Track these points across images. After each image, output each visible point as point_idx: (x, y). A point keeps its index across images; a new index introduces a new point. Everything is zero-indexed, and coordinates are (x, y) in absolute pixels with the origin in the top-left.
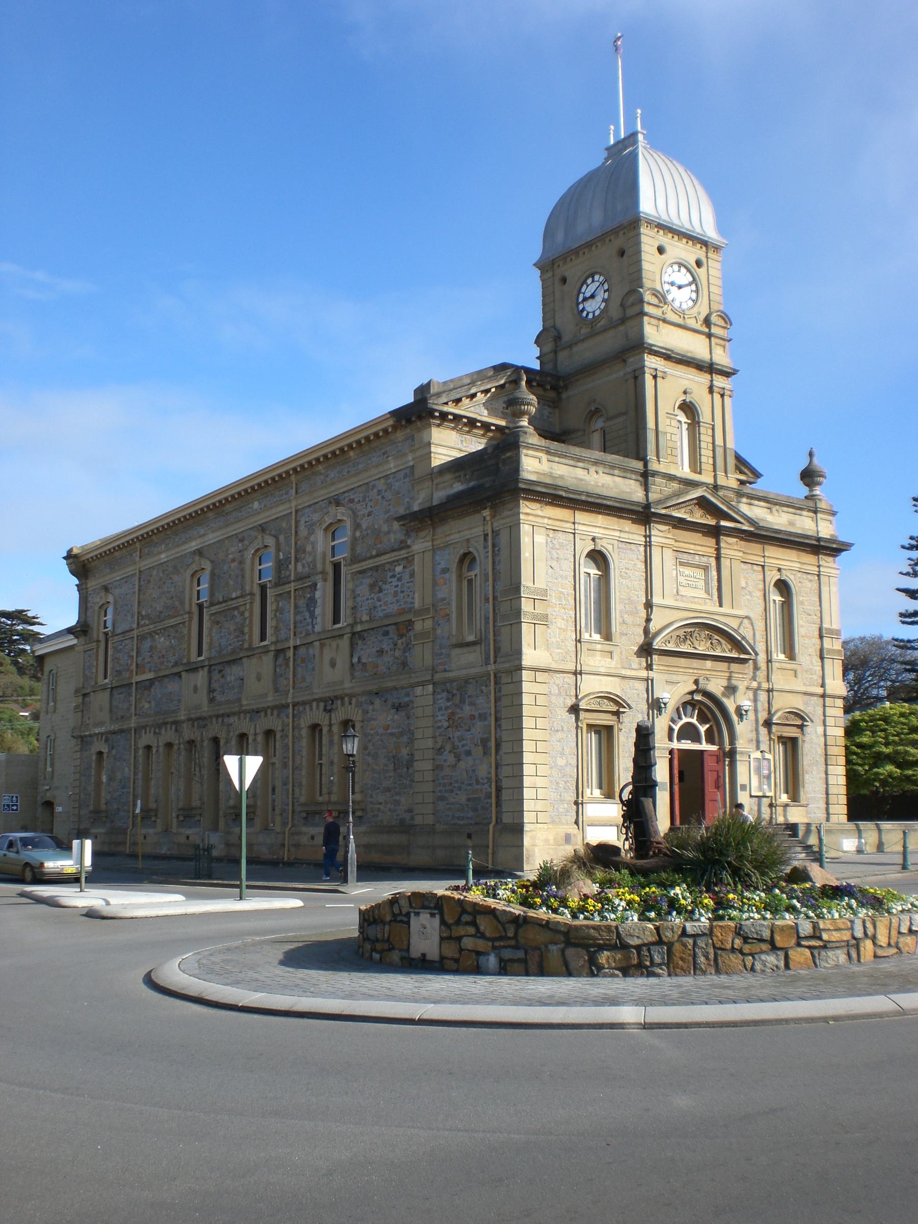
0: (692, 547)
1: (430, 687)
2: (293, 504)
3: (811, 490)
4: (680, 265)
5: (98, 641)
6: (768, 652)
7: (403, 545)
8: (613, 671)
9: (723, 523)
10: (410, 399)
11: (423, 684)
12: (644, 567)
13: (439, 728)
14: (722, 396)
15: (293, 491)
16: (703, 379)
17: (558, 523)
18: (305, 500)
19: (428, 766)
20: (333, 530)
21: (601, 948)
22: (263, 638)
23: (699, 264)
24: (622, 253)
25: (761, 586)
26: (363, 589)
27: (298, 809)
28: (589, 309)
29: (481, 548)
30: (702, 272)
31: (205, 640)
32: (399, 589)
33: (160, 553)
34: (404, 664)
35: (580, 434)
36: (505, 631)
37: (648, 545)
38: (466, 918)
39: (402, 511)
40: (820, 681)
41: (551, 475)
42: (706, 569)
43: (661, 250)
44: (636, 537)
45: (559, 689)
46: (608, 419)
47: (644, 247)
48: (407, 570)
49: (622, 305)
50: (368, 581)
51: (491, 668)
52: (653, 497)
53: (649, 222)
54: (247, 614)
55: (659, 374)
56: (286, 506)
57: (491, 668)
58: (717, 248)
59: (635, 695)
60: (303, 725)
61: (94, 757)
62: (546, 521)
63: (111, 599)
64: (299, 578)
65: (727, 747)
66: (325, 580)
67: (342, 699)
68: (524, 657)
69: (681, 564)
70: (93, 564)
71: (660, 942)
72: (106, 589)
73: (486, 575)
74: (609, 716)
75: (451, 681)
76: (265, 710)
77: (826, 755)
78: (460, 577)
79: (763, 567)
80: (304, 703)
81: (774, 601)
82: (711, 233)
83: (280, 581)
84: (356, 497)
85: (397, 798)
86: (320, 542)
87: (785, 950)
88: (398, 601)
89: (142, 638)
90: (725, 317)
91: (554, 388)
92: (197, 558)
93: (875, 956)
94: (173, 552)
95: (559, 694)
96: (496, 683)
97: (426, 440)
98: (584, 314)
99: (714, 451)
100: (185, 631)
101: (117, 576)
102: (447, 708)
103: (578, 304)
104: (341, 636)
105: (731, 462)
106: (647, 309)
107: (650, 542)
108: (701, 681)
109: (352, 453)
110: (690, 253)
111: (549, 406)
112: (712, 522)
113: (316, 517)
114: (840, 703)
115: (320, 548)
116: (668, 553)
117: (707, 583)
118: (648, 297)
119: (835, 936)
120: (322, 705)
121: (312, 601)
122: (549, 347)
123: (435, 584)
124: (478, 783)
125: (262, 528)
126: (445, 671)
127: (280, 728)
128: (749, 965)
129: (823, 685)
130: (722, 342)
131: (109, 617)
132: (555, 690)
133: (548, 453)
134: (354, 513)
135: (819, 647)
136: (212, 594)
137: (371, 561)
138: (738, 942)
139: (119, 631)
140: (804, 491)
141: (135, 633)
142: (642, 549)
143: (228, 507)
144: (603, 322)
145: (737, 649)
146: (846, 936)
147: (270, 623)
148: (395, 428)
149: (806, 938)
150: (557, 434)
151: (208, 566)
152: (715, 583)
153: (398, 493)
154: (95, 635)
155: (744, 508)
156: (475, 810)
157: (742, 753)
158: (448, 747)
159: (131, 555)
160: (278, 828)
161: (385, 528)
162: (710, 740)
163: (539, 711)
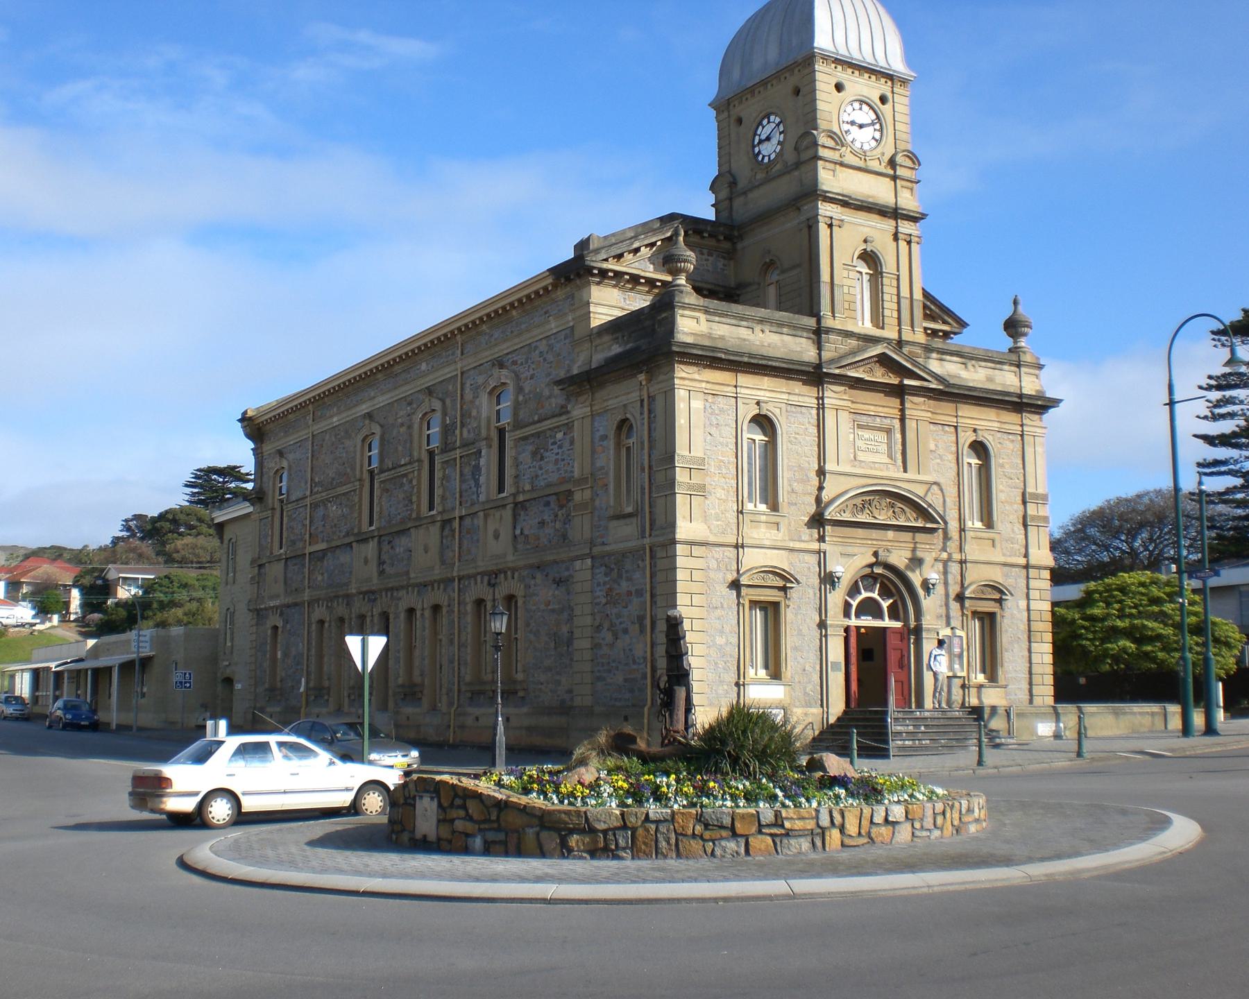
1: (589, 561)
2: (459, 365)
3: (1015, 342)
4: (862, 102)
5: (273, 509)
6: (961, 520)
7: (563, 411)
8: (779, 544)
9: (906, 382)
10: (569, 254)
11: (582, 558)
13: (597, 604)
14: (909, 243)
15: (459, 352)
16: (888, 225)
17: (717, 387)
18: (470, 362)
19: (586, 644)
20: (497, 394)
21: (571, 832)
22: (431, 508)
23: (883, 100)
24: (797, 92)
25: (954, 449)
26: (526, 457)
27: (463, 688)
28: (764, 152)
29: (638, 416)
30: (887, 109)
31: (376, 509)
32: (559, 457)
33: (332, 417)
34: (564, 537)
35: (754, 287)
36: (660, 503)
37: (821, 407)
38: (458, 802)
39: (562, 374)
40: (1023, 551)
41: (710, 336)
42: (889, 431)
43: (839, 87)
44: (807, 399)
45: (718, 563)
46: (783, 272)
47: (819, 85)
48: (568, 437)
49: (796, 149)
50: (530, 448)
51: (647, 541)
52: (826, 355)
53: (825, 58)
54: (415, 482)
55: (835, 222)
56: (453, 367)
57: (647, 541)
58: (904, 82)
59: (805, 569)
60: (468, 600)
61: (269, 632)
62: (704, 385)
63: (285, 464)
64: (465, 445)
65: (912, 624)
66: (490, 446)
67: (505, 573)
68: (678, 530)
69: (860, 427)
70: (268, 427)
71: (624, 827)
72: (281, 453)
73: (642, 443)
74: (775, 592)
75: (609, 554)
76: (432, 583)
77: (1029, 631)
78: (618, 445)
79: (956, 427)
80: (469, 577)
81: (970, 464)
82: (897, 64)
83: (446, 448)
84: (520, 358)
85: (558, 677)
86: (484, 405)
87: (747, 837)
88: (559, 469)
89: (315, 506)
90: (913, 157)
91: (728, 238)
92: (367, 422)
93: (843, 845)
94: (344, 415)
95: (719, 568)
96: (651, 558)
97: (585, 299)
98: (760, 158)
99: (899, 303)
100: (356, 499)
101: (292, 439)
102: (605, 583)
103: (754, 147)
104: (504, 506)
105: (918, 313)
106: (822, 152)
108: (880, 552)
109: (514, 313)
110: (872, 89)
111: (724, 258)
112: (894, 380)
113: (480, 380)
114: (1046, 574)
115: (484, 415)
116: (844, 417)
117: (890, 447)
118: (823, 140)
119: (799, 825)
120: (486, 578)
121: (477, 468)
122: (724, 193)
123: (593, 452)
124: (634, 662)
125: (429, 391)
126: (603, 544)
127: (446, 603)
128: (709, 851)
129: (1026, 556)
130: (909, 184)
131: (284, 483)
132: (713, 564)
133: (706, 312)
134: (517, 376)
135: (1021, 514)
136: (382, 461)
137: (533, 427)
138: (699, 828)
139: (293, 498)
140: (1009, 342)
141: (308, 501)
142: (814, 412)
143: (397, 369)
144: (778, 167)
145: (923, 517)
146: (811, 824)
147: (438, 492)
148: (555, 286)
149: (768, 826)
150: (722, 291)
151: (377, 429)
152: (899, 447)
153: (559, 355)
154: (270, 501)
155: (935, 365)
156: (631, 691)
157: (928, 630)
158: (606, 625)
159: (305, 417)
160: (444, 709)
161: (546, 392)
162: (894, 614)
163: (695, 587)
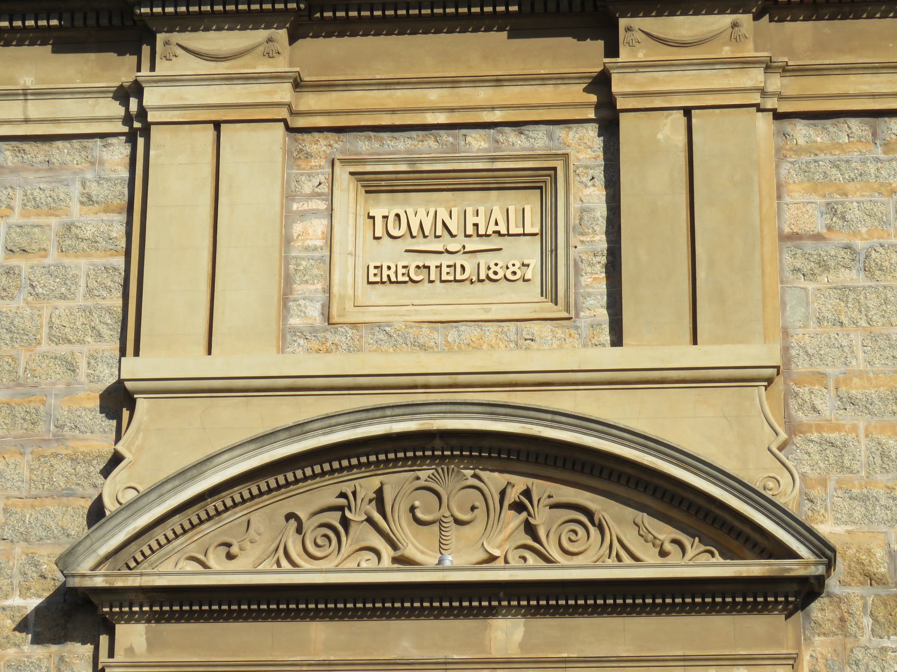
0: (434, 96)
12: (119, 231)
37: (138, 129)
42: (541, 180)
69: (373, 184)
107: (142, 113)
116: (256, 153)
117: (549, 253)
142: (119, 151)
